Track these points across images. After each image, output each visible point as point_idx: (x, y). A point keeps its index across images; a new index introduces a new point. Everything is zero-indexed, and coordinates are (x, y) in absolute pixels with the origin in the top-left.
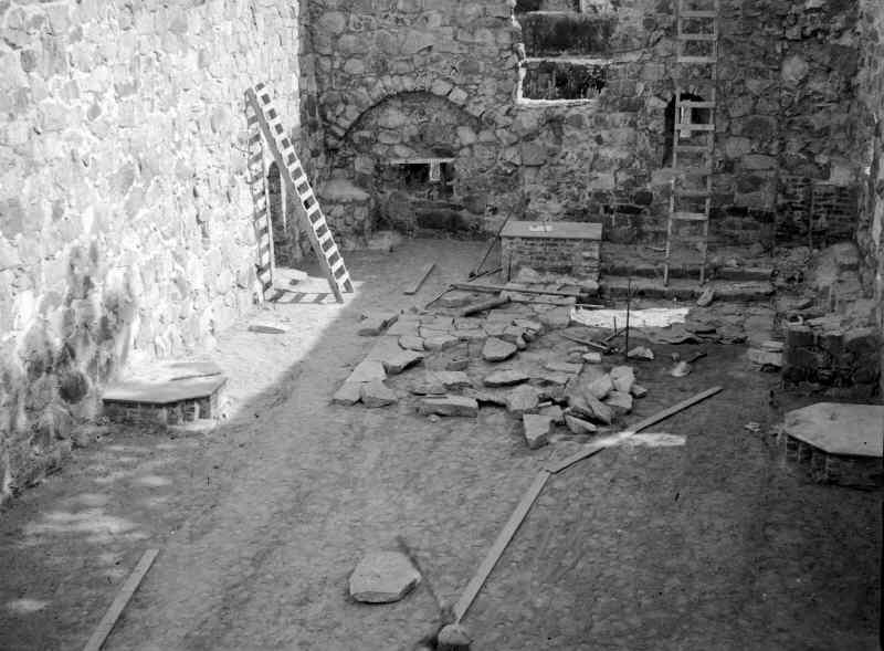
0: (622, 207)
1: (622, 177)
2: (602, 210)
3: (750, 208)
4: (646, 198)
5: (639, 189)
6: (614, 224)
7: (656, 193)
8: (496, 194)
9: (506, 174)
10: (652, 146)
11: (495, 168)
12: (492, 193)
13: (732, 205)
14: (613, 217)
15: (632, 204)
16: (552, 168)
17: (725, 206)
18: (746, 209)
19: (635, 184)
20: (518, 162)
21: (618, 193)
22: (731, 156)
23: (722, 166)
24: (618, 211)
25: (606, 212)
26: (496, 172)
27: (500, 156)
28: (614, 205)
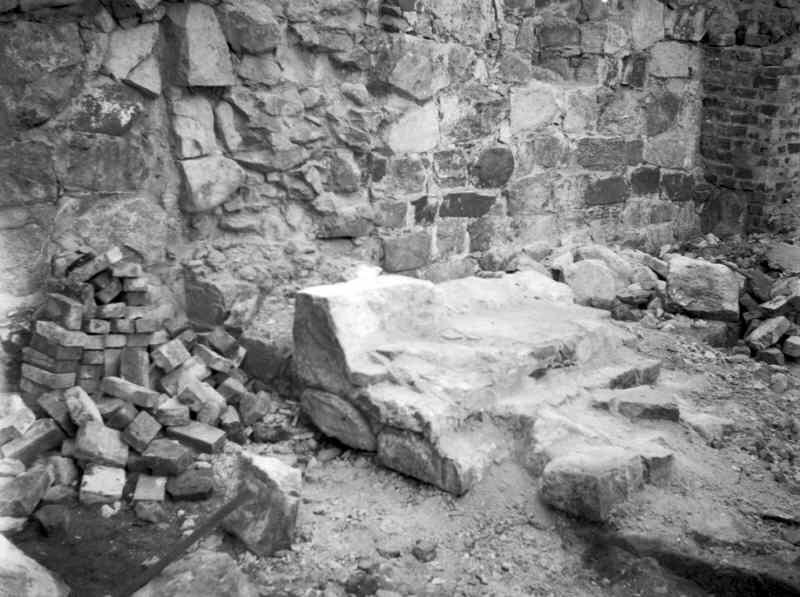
0: (453, 197)
1: (454, 109)
2: (410, 217)
3: (663, 171)
4: (496, 169)
5: (486, 143)
6: (435, 250)
7: (519, 151)
8: (83, 210)
9: (113, 128)
10: (507, 14)
11: (77, 108)
12: (68, 203)
13: (640, 165)
14: (433, 230)
15: (470, 188)
16: (266, 96)
17: (631, 170)
18: (656, 173)
19: (477, 128)
20: (151, 81)
21: (444, 156)
22: (640, 46)
23: (629, 68)
24: (444, 213)
25: (418, 219)
26: (82, 121)
27: (92, 67)
28: (436, 196)
